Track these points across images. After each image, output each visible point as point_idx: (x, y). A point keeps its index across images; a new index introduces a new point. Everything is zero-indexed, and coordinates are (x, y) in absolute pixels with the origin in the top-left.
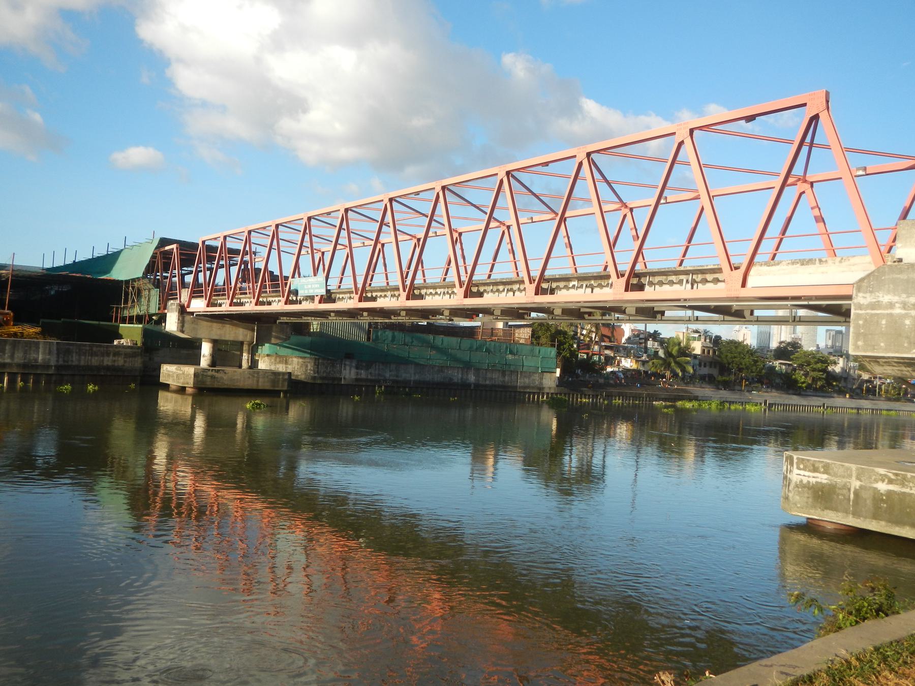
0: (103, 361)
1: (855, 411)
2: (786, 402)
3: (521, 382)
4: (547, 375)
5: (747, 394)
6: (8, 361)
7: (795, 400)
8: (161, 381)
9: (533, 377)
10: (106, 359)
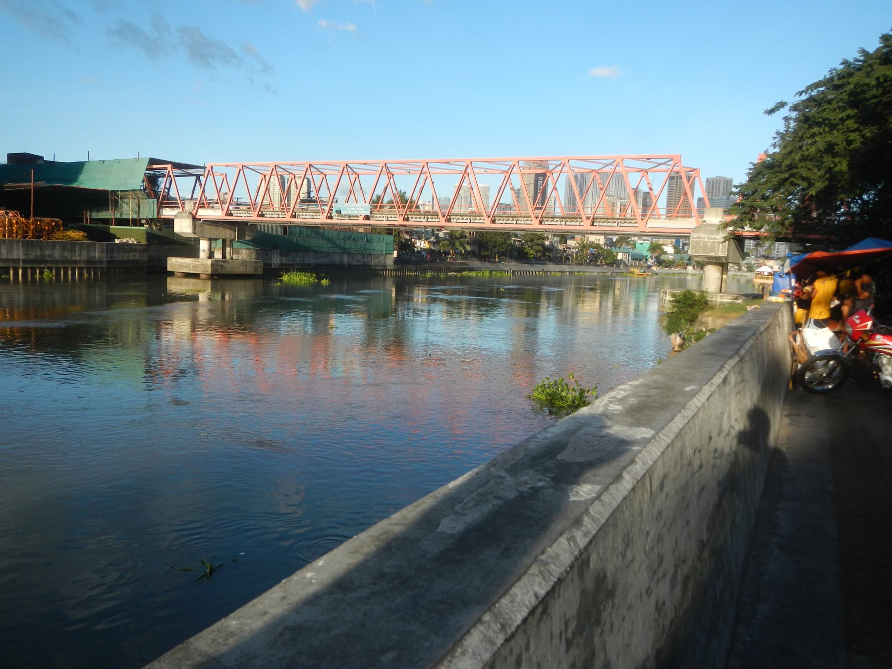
0: (129, 257)
1: (558, 274)
2: (522, 269)
3: (373, 261)
4: (388, 256)
5: (499, 264)
6: (78, 258)
7: (526, 267)
8: (169, 269)
9: (380, 258)
10: (131, 254)
